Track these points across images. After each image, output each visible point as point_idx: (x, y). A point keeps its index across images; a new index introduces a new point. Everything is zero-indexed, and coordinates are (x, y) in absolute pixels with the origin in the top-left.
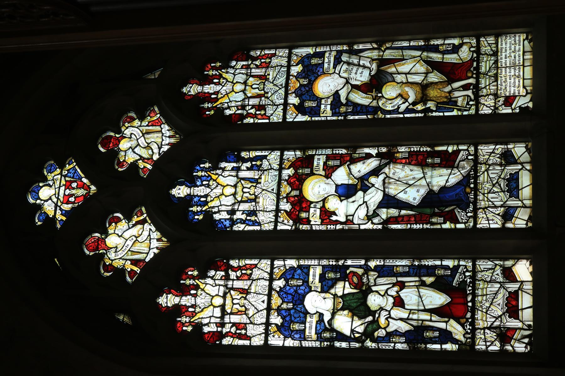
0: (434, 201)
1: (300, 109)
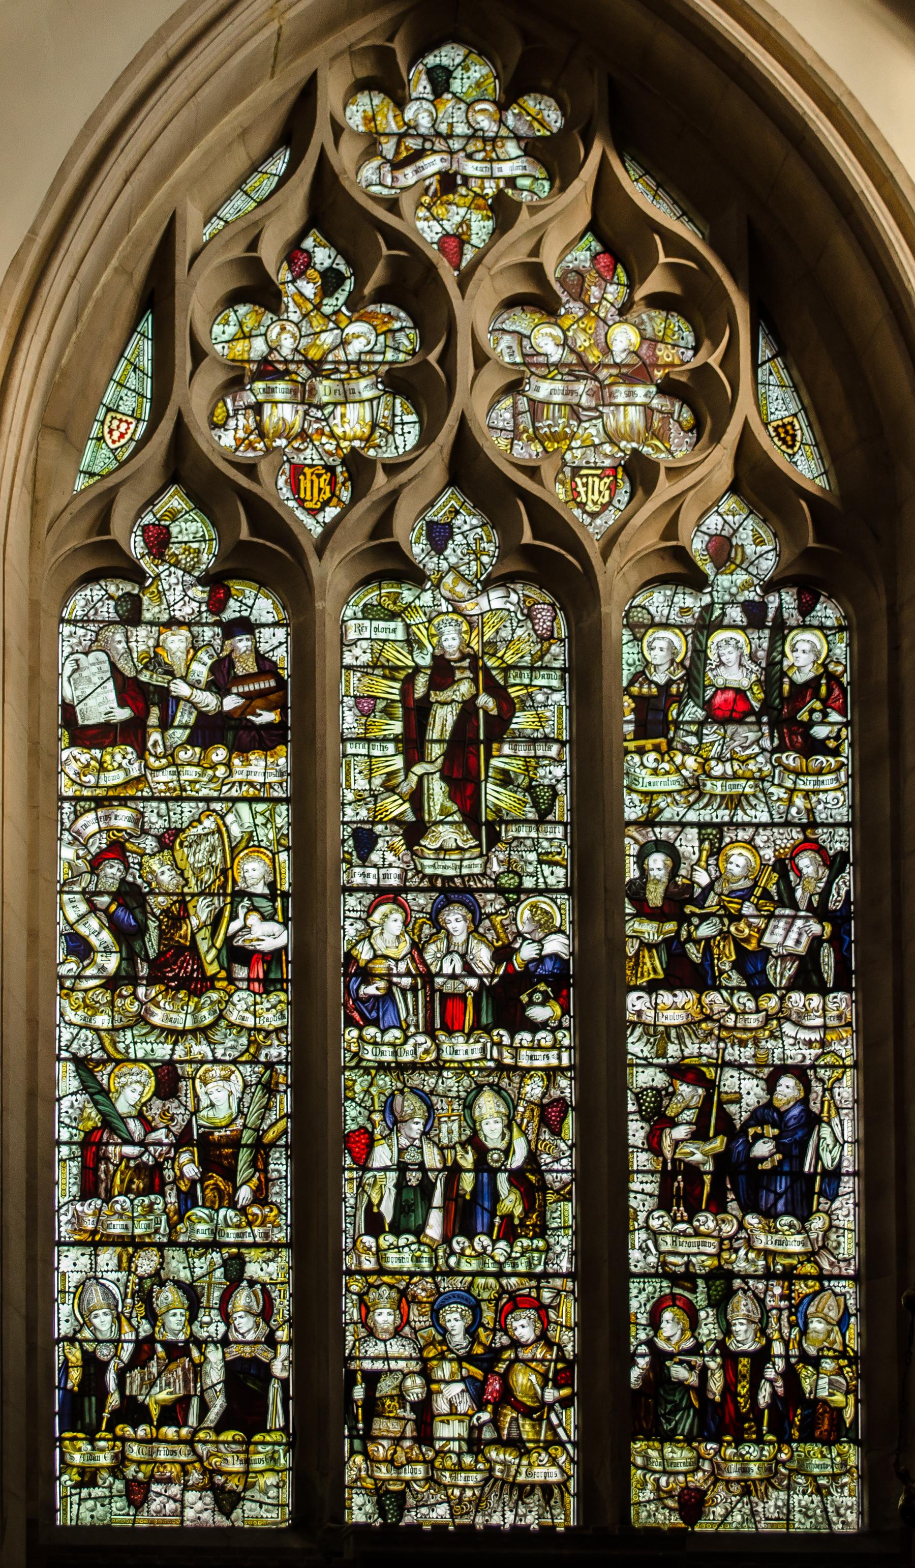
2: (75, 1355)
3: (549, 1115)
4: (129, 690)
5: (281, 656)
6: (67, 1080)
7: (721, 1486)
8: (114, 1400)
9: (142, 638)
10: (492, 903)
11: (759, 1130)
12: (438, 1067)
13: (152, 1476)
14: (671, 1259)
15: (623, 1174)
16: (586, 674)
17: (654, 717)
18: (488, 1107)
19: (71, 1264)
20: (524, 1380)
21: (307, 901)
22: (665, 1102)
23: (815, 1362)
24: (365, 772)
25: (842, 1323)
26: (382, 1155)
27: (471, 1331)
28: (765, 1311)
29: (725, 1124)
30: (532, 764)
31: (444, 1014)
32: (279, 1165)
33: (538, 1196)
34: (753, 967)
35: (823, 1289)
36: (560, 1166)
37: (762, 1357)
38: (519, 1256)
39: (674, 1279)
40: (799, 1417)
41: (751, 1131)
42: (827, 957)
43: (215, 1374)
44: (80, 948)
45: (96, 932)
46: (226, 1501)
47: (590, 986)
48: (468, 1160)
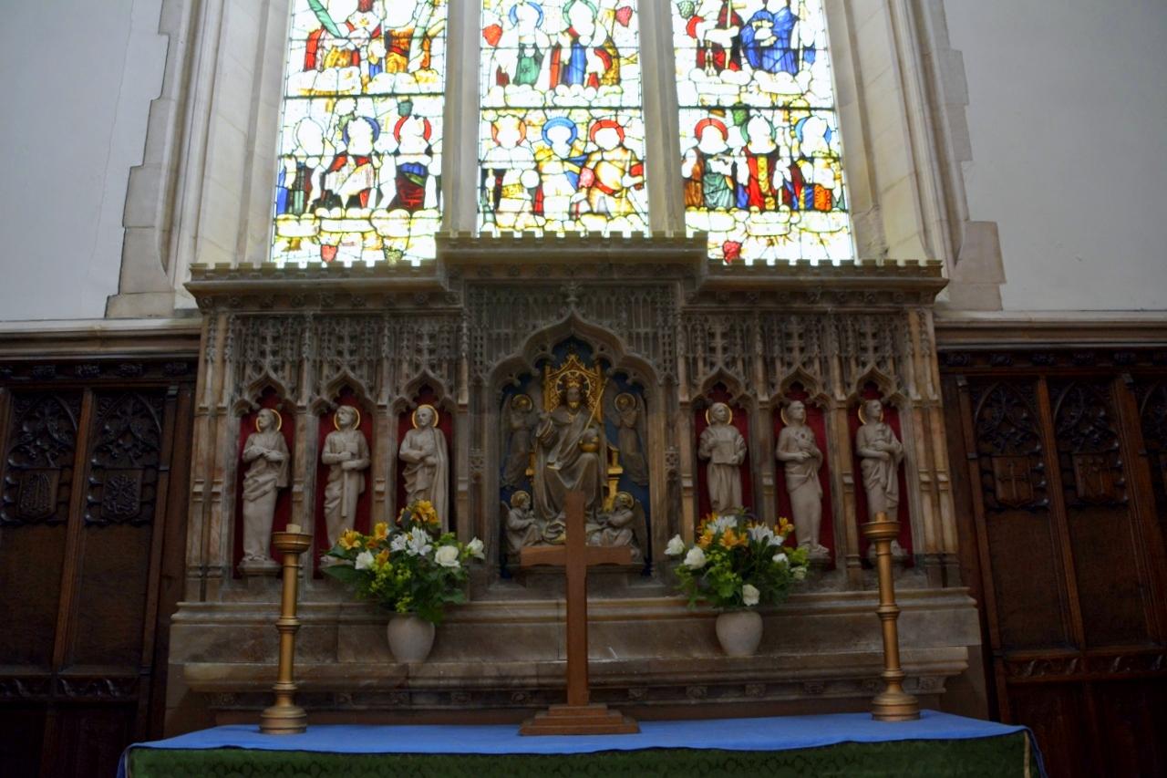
2: (291, 165)
7: (752, 239)
8: (316, 193)
11: (759, 23)
13: (340, 241)
14: (705, 97)
15: (668, 51)
19: (292, 111)
20: (610, 176)
22: (697, 8)
23: (811, 160)
25: (827, 135)
26: (509, 39)
27: (570, 143)
28: (773, 130)
29: (737, 20)
32: (438, 47)
33: (615, 61)
35: (811, 116)
36: (627, 39)
37: (773, 157)
39: (710, 109)
41: (754, 24)
48: (566, 41)
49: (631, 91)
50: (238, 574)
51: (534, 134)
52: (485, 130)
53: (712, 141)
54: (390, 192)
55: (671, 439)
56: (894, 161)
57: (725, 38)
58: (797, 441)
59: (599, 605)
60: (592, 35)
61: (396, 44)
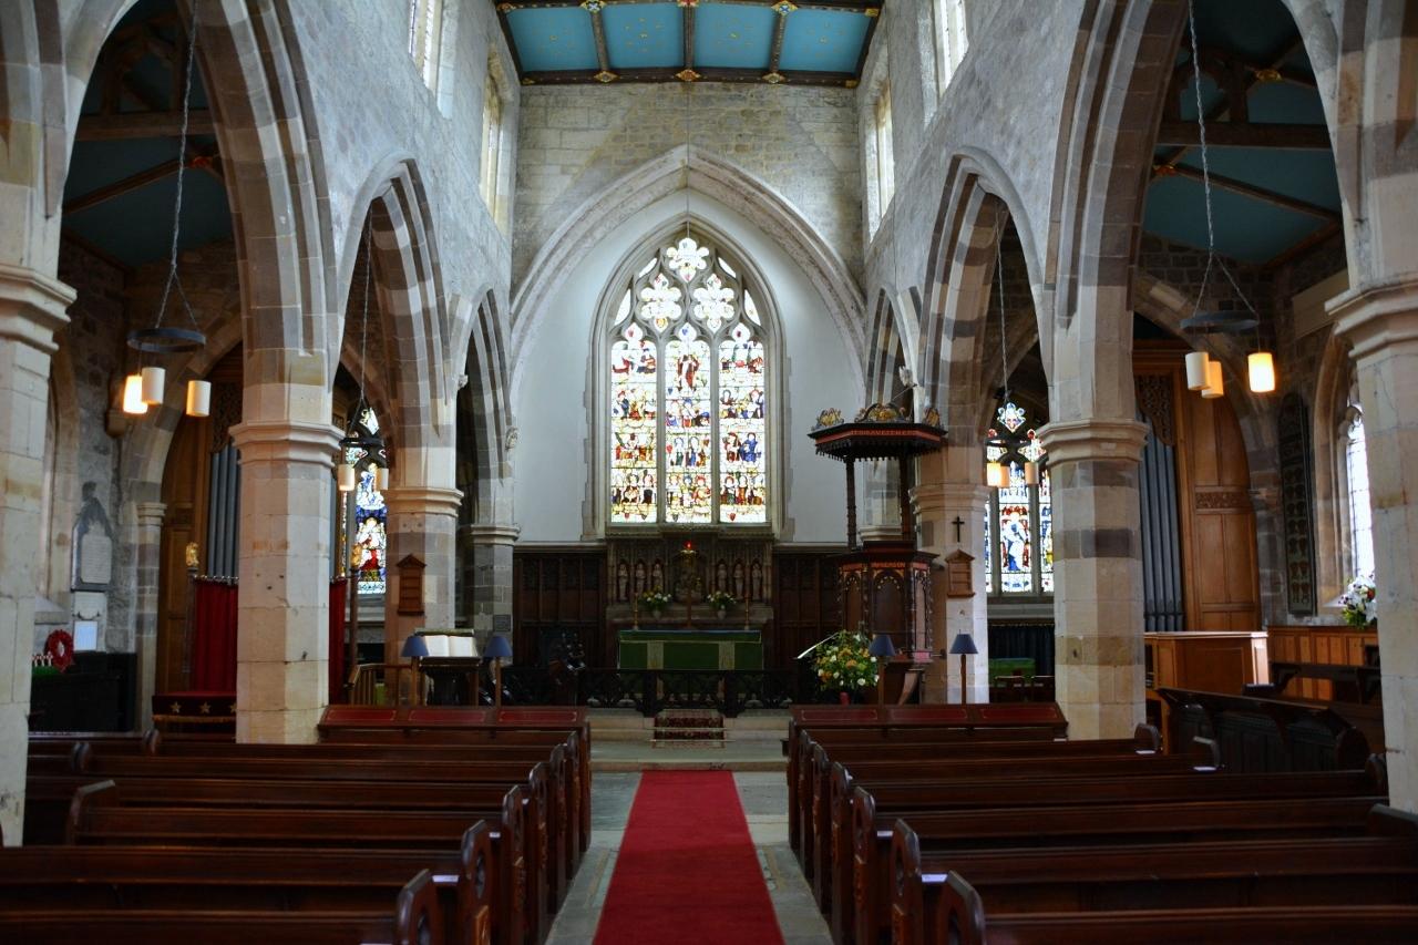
0: (1010, 559)
1: (1045, 509)
3: (706, 443)
4: (626, 362)
5: (655, 357)
6: (613, 437)
9: (628, 352)
10: (694, 402)
12: (684, 434)
16: (714, 358)
17: (726, 366)
18: (694, 442)
19: (614, 472)
20: (701, 494)
21: (661, 401)
24: (671, 378)
26: (674, 450)
29: (739, 444)
30: (702, 375)
31: (686, 423)
32: (654, 452)
34: (744, 413)
36: (708, 451)
37: (746, 488)
38: (700, 469)
40: (753, 500)
42: (759, 412)
43: (642, 493)
44: (616, 411)
45: (619, 408)
46: (644, 517)
47: (713, 418)
48: (690, 451)
49: (708, 468)
50: (619, 601)
51: (681, 481)
52: (668, 479)
53: (729, 484)
54: (642, 498)
55: (710, 572)
56: (774, 499)
57: (735, 450)
58: (738, 573)
59: (694, 608)
60: (698, 450)
61: (642, 451)
